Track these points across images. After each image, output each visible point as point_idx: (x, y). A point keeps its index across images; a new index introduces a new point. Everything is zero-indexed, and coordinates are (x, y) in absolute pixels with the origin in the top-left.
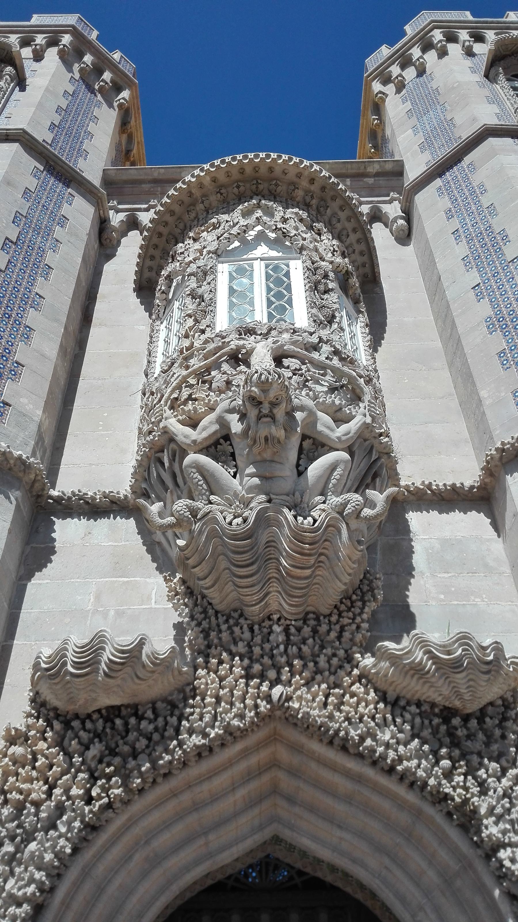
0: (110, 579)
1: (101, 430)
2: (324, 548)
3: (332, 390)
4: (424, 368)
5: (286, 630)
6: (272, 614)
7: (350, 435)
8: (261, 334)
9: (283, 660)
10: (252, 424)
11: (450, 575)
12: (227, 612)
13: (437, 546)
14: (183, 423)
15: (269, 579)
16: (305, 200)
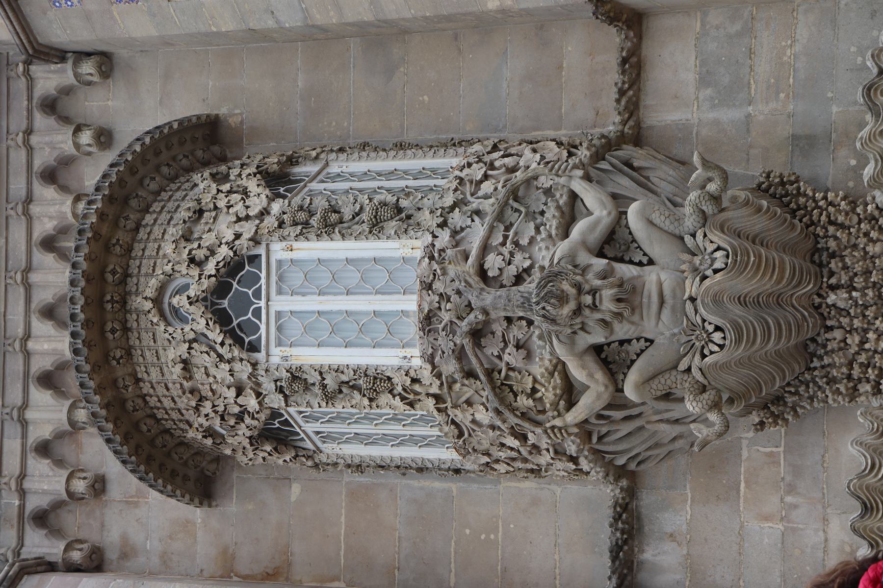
0: (741, 505)
1: (496, 536)
2: (747, 239)
3: (531, 215)
4: (402, 69)
5: (833, 288)
6: (813, 304)
7: (603, 198)
8: (439, 302)
9: (870, 293)
10: (598, 316)
11: (752, 81)
12: (807, 356)
13: (709, 92)
14: (570, 405)
15: (779, 304)
16: (131, 230)
